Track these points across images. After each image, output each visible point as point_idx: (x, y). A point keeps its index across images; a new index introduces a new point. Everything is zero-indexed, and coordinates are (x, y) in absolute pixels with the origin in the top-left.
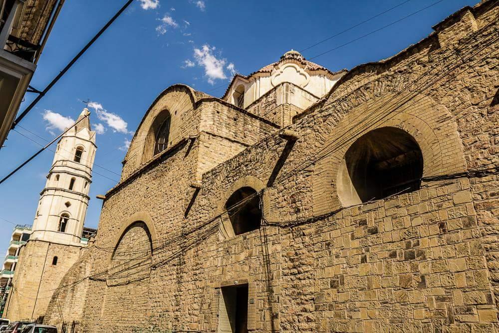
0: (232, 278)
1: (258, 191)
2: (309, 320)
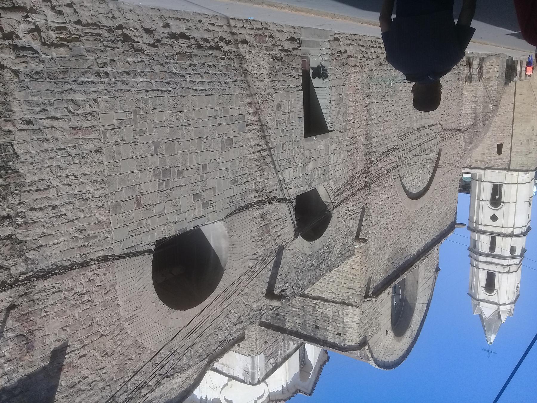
0: (319, 142)
1: (300, 237)
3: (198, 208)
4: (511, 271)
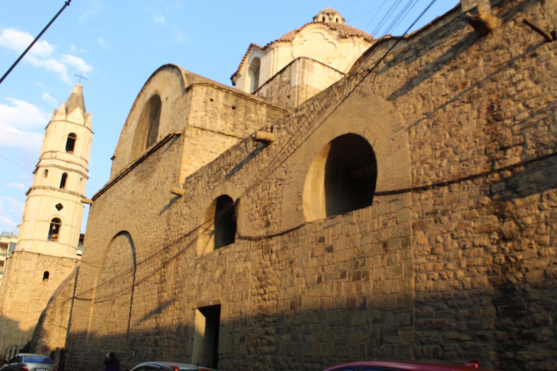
1: (234, 200)
2: (270, 343)
3: (329, 238)
4: (50, 153)
